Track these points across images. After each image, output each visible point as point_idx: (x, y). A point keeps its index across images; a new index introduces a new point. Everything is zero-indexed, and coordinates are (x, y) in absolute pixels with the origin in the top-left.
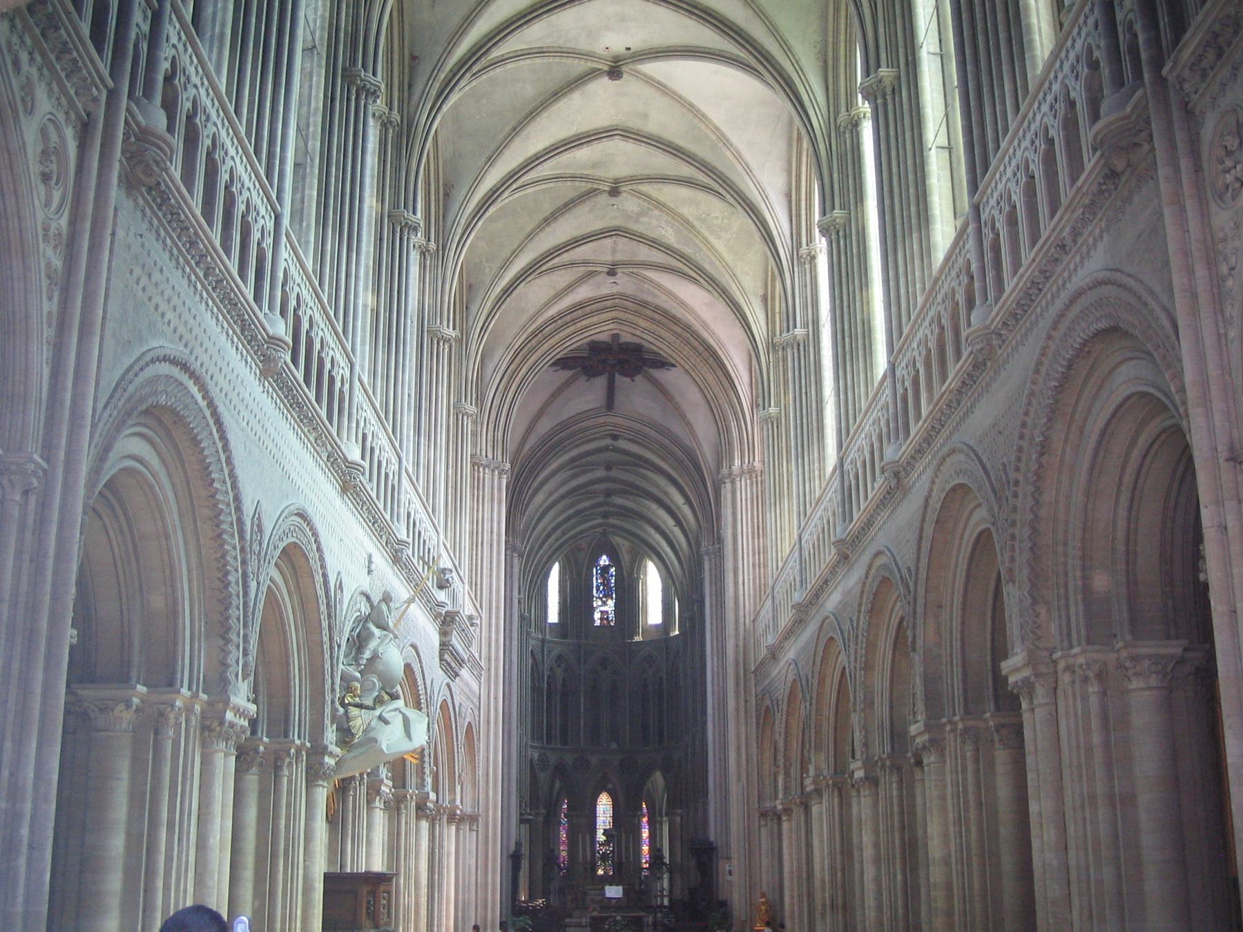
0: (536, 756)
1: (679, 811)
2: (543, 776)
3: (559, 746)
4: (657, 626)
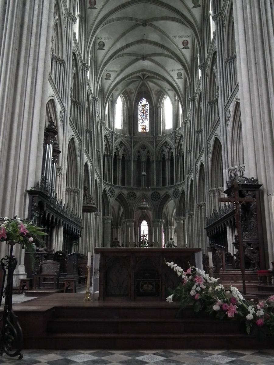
0: (107, 188)
1: (182, 218)
2: (112, 200)
3: (120, 185)
4: (170, 130)
